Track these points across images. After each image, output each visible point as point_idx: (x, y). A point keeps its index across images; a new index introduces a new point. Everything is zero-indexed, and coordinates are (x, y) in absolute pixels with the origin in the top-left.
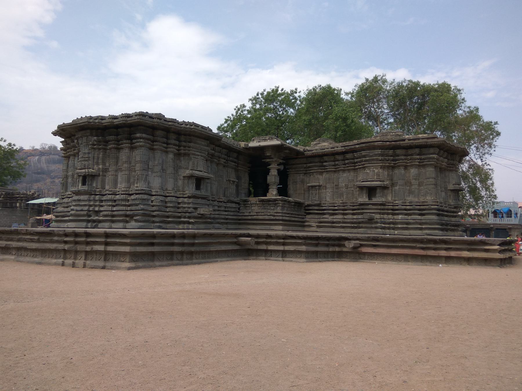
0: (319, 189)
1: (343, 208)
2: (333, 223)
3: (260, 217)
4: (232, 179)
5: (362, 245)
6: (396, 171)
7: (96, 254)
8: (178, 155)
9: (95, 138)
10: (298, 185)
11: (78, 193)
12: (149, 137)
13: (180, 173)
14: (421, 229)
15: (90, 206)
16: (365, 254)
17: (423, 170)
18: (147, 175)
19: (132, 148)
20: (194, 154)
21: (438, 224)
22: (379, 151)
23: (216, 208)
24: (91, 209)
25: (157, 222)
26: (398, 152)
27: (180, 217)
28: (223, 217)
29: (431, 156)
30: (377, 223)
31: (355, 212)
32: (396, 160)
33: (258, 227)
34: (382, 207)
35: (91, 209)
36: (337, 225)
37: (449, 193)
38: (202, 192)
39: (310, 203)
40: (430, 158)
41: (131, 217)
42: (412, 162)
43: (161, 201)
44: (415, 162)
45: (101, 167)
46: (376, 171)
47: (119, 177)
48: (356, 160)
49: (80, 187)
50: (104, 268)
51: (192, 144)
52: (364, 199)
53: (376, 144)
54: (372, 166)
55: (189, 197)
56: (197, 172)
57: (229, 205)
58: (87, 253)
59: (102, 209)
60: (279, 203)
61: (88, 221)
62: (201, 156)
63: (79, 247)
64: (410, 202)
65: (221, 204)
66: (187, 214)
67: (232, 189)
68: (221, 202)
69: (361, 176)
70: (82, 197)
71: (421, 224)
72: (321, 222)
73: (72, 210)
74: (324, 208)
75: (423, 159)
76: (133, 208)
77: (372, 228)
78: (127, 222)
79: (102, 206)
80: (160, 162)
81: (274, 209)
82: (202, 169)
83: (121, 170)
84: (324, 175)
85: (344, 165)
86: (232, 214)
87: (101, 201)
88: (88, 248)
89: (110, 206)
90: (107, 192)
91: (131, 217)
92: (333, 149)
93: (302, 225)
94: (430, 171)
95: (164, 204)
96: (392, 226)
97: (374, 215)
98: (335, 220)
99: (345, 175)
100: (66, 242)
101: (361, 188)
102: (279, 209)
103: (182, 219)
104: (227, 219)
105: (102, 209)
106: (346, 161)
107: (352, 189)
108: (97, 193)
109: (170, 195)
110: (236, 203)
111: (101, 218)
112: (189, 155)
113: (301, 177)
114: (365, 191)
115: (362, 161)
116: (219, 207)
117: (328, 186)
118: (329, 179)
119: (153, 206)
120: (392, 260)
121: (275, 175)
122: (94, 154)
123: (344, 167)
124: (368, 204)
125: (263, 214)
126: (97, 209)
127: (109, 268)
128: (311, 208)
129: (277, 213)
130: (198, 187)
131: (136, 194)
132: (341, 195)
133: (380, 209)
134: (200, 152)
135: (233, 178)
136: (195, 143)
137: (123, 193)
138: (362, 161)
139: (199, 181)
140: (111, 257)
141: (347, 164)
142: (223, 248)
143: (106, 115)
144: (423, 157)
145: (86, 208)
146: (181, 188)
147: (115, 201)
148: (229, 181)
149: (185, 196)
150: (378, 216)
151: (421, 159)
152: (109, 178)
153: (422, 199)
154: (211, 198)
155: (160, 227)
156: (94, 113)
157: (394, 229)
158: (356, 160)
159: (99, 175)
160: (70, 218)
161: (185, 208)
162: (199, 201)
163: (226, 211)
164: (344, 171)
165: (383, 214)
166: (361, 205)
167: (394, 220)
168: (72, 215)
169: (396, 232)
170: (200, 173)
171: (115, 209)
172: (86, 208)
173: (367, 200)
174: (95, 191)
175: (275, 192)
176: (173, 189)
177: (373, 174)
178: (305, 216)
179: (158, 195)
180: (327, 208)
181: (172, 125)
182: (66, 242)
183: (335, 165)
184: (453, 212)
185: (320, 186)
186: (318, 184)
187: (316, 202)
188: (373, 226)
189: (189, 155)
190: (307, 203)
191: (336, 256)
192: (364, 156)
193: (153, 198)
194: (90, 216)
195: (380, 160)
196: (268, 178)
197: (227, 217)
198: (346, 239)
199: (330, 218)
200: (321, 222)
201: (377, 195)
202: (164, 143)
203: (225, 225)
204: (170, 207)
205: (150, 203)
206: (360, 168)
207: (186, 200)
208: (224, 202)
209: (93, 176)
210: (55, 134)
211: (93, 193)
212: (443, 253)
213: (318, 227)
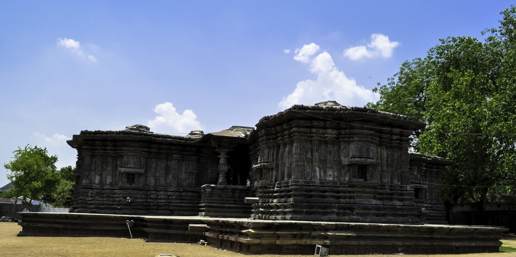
55: (120, 189)
65: (172, 193)
82: (133, 166)
104: (181, 206)
116: (168, 196)
139: (131, 177)
161: (116, 197)
163: (180, 199)
170: (128, 170)
202: (103, 150)
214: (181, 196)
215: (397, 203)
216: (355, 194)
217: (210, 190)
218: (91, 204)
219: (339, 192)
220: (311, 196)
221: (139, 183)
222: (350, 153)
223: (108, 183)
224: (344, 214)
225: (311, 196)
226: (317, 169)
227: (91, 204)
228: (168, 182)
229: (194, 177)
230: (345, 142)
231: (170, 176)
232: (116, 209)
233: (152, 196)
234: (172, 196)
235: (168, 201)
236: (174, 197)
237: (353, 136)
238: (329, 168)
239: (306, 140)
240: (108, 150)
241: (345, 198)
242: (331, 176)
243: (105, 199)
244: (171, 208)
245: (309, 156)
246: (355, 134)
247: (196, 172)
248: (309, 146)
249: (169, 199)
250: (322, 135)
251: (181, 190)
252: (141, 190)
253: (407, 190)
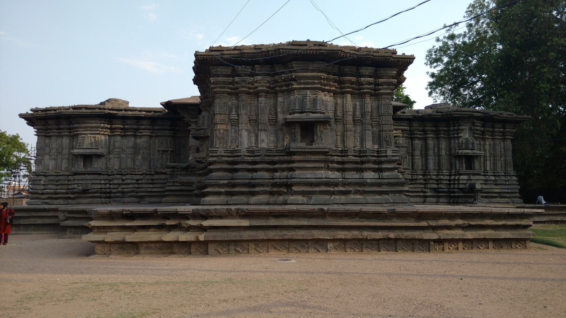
20: (83, 134)
27: (67, 193)
51: (76, 125)
57: (156, 177)
65: (141, 177)
112: (78, 135)
134: (92, 131)
139: (87, 158)
142: (40, 221)
161: (71, 184)
163: (153, 184)
189: (78, 135)
197: (149, 190)
202: (57, 129)
214: (153, 180)
215: (369, 176)
216: (295, 165)
218: (43, 194)
219: (274, 163)
220: (236, 170)
221: (98, 165)
222: (287, 107)
223: (63, 169)
224: (280, 194)
225: (236, 170)
226: (245, 134)
227: (43, 194)
228: (137, 163)
229: (169, 156)
230: (282, 92)
231: (140, 157)
232: (69, 198)
233: (116, 182)
234: (141, 179)
235: (136, 186)
236: (143, 182)
237: (292, 82)
238: (261, 130)
239: (230, 94)
240: (62, 129)
241: (283, 170)
242: (266, 141)
243: (59, 187)
244: (140, 194)
245: (234, 116)
246: (294, 80)
247: (171, 149)
248: (235, 102)
249: (138, 184)
250: (250, 86)
251: (153, 173)
252: (100, 174)
253: (386, 156)
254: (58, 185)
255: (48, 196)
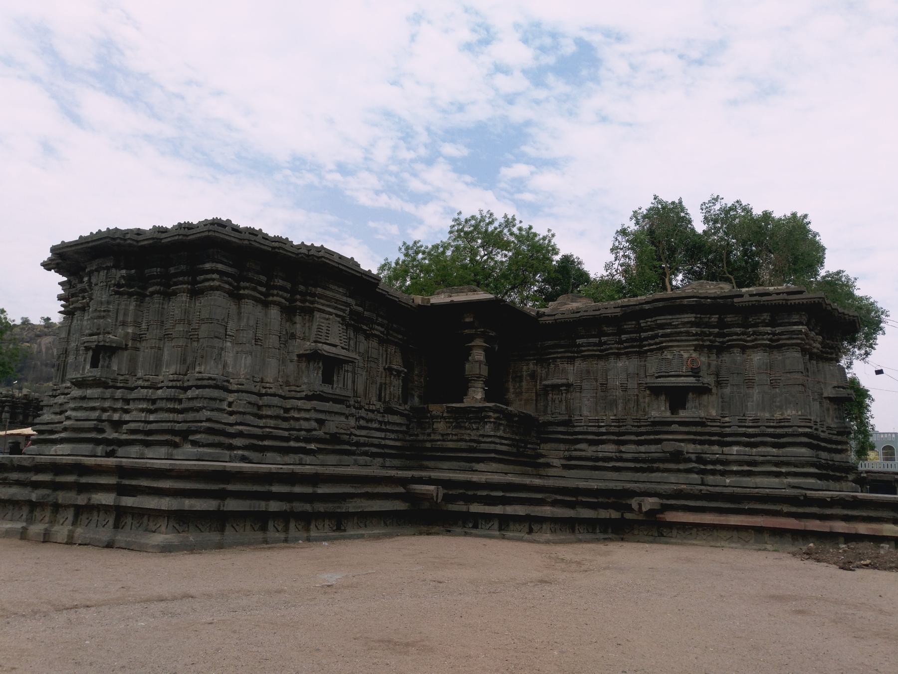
0: (567, 391)
1: (617, 430)
2: (597, 459)
3: (451, 445)
4: (395, 367)
5: (665, 508)
6: (726, 357)
7: (99, 512)
8: (289, 312)
9: (124, 272)
10: (524, 384)
11: (80, 384)
12: (229, 270)
13: (291, 348)
14: (778, 475)
15: (104, 410)
16: (672, 525)
17: (777, 356)
18: (222, 349)
19: (195, 294)
20: (323, 311)
21: (813, 465)
22: (690, 317)
23: (362, 423)
24: (105, 416)
25: (239, 448)
26: (729, 319)
27: (287, 439)
28: (376, 441)
29: (795, 327)
30: (689, 460)
31: (643, 438)
32: (724, 335)
33: (446, 465)
34: (699, 429)
35: (105, 416)
36: (606, 464)
37: (826, 404)
38: (337, 389)
39: (549, 418)
40: (793, 332)
41: (185, 435)
42: (756, 340)
43: (249, 403)
44: (763, 339)
45: (130, 330)
46: (686, 355)
47: (166, 353)
48: (643, 335)
49: (88, 372)
50: (110, 545)
51: (319, 290)
52: (659, 411)
53: (685, 301)
54: (678, 346)
55: (308, 398)
56: (326, 347)
58: (79, 511)
59: (127, 417)
60: (489, 417)
61: (98, 442)
62: (337, 315)
63: (62, 497)
64: (754, 421)
65: (371, 415)
66: (303, 433)
67: (395, 387)
68: (373, 411)
69: (653, 364)
70: (89, 392)
71: (777, 464)
72: (570, 458)
73: (68, 418)
74: (577, 429)
75: (779, 334)
76: (190, 416)
77: (679, 471)
78: (176, 445)
79: (127, 411)
80: (252, 322)
81: (478, 429)
82: (337, 342)
83: (167, 337)
84: (577, 364)
85: (617, 343)
86: (392, 436)
87: (127, 401)
88: (81, 500)
89: (142, 410)
90: (140, 383)
91: (185, 435)
92: (598, 313)
93: (534, 463)
94: (793, 357)
95: (255, 410)
96: (719, 467)
97: (682, 444)
98: (600, 455)
99: (620, 364)
100: (36, 485)
101: (656, 391)
102: (488, 429)
103: (292, 444)
105: (127, 417)
106: (624, 337)
107: (636, 392)
108: (119, 385)
109: (269, 391)
110: (402, 415)
111: (124, 437)
113: (531, 366)
114: (663, 397)
115: (656, 336)
117: (585, 385)
118: (588, 372)
119: (231, 413)
120: (731, 539)
121: (480, 362)
122: (119, 304)
123: (618, 349)
124: (670, 423)
125: (455, 438)
126: (116, 417)
127: (123, 545)
128: (551, 429)
129: (483, 436)
130: (327, 379)
131: (198, 387)
132: (614, 403)
133: (695, 434)
134: (335, 308)
135: (397, 364)
136: (325, 288)
137: (170, 384)
138: (656, 336)
139: (331, 366)
140: (129, 520)
141: (625, 341)
143: (147, 226)
144: (778, 330)
145: (95, 414)
146: (291, 379)
147: (154, 401)
148: (389, 370)
149: (299, 395)
150: (691, 447)
151: (774, 334)
152: (145, 352)
153: (778, 416)
154: (352, 403)
155: (244, 459)
156: (126, 223)
157: (723, 473)
158: (643, 335)
159: (126, 348)
160: (63, 435)
161: (297, 419)
162: (328, 406)
164: (618, 356)
165: (702, 443)
166: (654, 424)
167: (724, 457)
168: (65, 429)
169: (728, 481)
171: (152, 418)
172: (95, 414)
173: (668, 414)
174: (115, 380)
175: (479, 396)
176: (276, 380)
177: (679, 361)
178: (539, 445)
179: (242, 392)
180: (584, 429)
181: (279, 248)
182: (36, 485)
183: (600, 344)
184: (840, 443)
185: (569, 386)
186: (564, 381)
187: (560, 418)
188: (682, 466)
190: (542, 419)
191: (610, 531)
192: (662, 326)
193: (231, 398)
194: (102, 431)
195: (694, 335)
196: (467, 366)
197: (383, 442)
198: (633, 494)
199: (590, 451)
200: (570, 458)
201: (688, 405)
203: (380, 460)
204: (267, 417)
205: (225, 406)
206: (651, 350)
207: (300, 403)
208: (379, 412)
209: (111, 350)
210: (47, 266)
211: (111, 384)
212: (840, 527)
213: (565, 467)
217: (496, 415)
243: (272, 423)
254: (261, 417)
255: (247, 442)
